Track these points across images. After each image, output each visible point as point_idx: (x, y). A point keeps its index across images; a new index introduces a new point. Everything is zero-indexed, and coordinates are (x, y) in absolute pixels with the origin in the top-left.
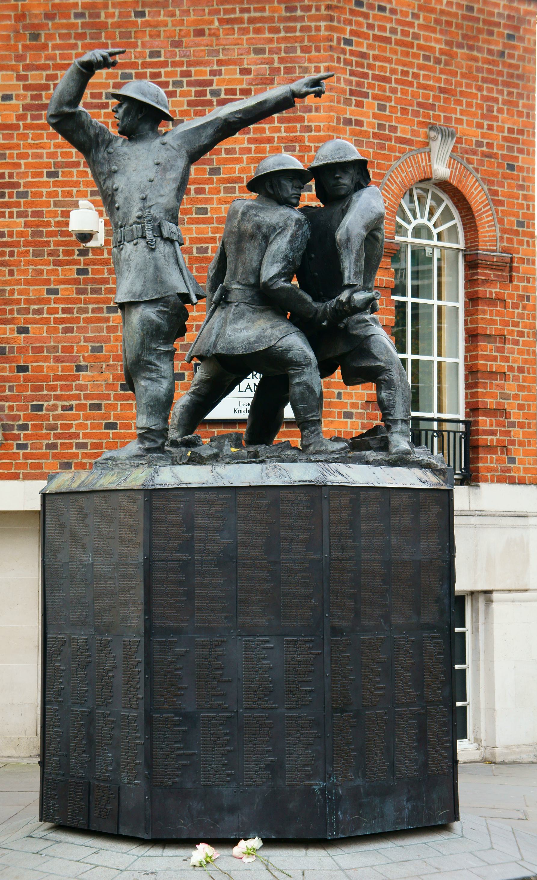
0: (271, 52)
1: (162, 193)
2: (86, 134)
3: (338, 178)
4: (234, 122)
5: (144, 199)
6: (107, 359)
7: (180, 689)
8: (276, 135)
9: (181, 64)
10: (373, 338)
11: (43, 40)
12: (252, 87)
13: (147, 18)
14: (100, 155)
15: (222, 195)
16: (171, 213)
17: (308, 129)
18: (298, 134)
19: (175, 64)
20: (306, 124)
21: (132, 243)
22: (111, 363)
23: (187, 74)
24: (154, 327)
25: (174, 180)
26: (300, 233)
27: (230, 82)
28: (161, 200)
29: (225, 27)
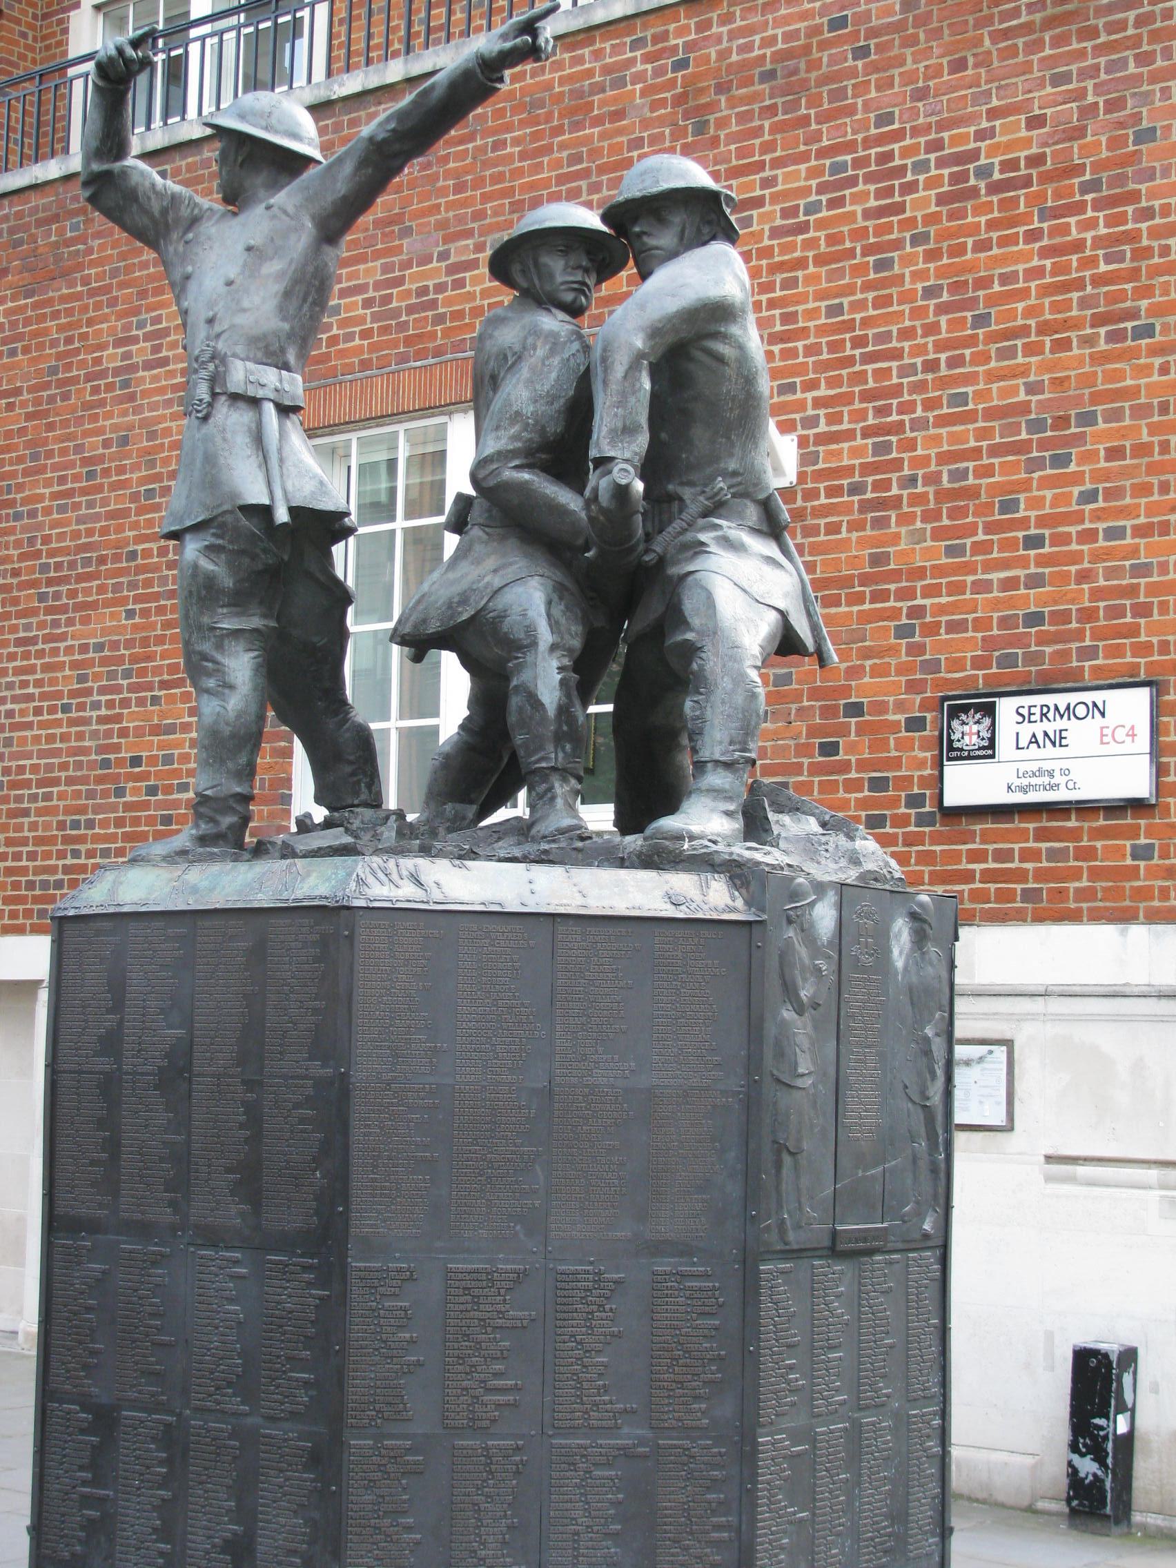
0: (1083, 74)
1: (246, 304)
2: (146, 212)
3: (639, 235)
4: (385, 141)
5: (210, 321)
6: (798, 696)
7: (93, 1353)
8: (1088, 236)
9: (927, 129)
10: (690, 578)
11: (712, 131)
12: (1048, 150)
13: (873, 57)
14: (171, 249)
16: (261, 345)
17: (1147, 214)
18: (1130, 226)
19: (916, 132)
20: (1144, 204)
22: (806, 703)
23: (937, 145)
24: (200, 579)
25: (280, 275)
26: (556, 361)
27: (1010, 146)
28: (241, 320)
29: (1002, 45)
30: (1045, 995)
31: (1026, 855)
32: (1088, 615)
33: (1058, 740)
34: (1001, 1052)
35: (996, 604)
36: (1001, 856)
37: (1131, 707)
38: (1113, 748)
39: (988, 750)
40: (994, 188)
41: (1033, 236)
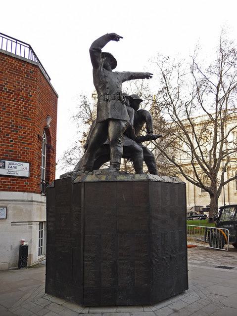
17: (30, 105)
30: (10, 201)
31: (8, 182)
32: (19, 152)
33: (15, 168)
34: (5, 209)
35: (5, 148)
36: (4, 182)
37: (27, 165)
41: (13, 101)
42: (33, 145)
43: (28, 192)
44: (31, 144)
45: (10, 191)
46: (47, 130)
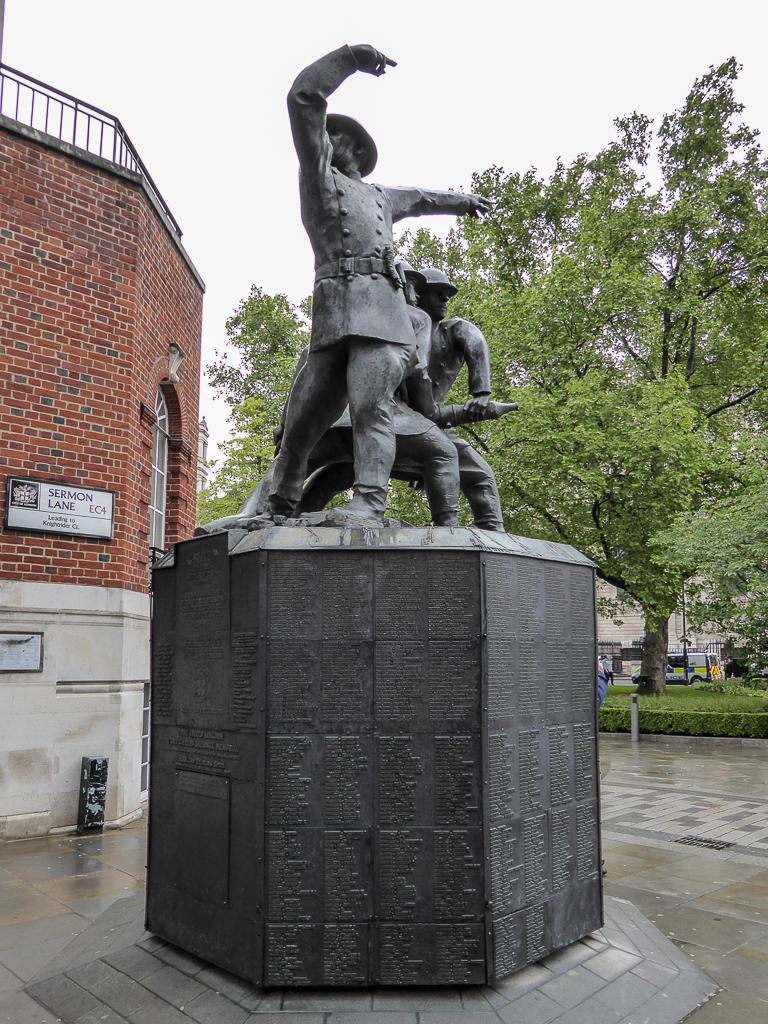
15: (41, 338)
21: (369, 277)
27: (53, 249)
30: (53, 613)
31: (49, 553)
32: (84, 458)
33: (70, 507)
34: (37, 638)
36: (35, 551)
37: (104, 500)
38: (95, 515)
39: (35, 504)
40: (45, 262)
42: (126, 434)
43: (108, 585)
44: (119, 433)
45: (54, 580)
46: (168, 391)
